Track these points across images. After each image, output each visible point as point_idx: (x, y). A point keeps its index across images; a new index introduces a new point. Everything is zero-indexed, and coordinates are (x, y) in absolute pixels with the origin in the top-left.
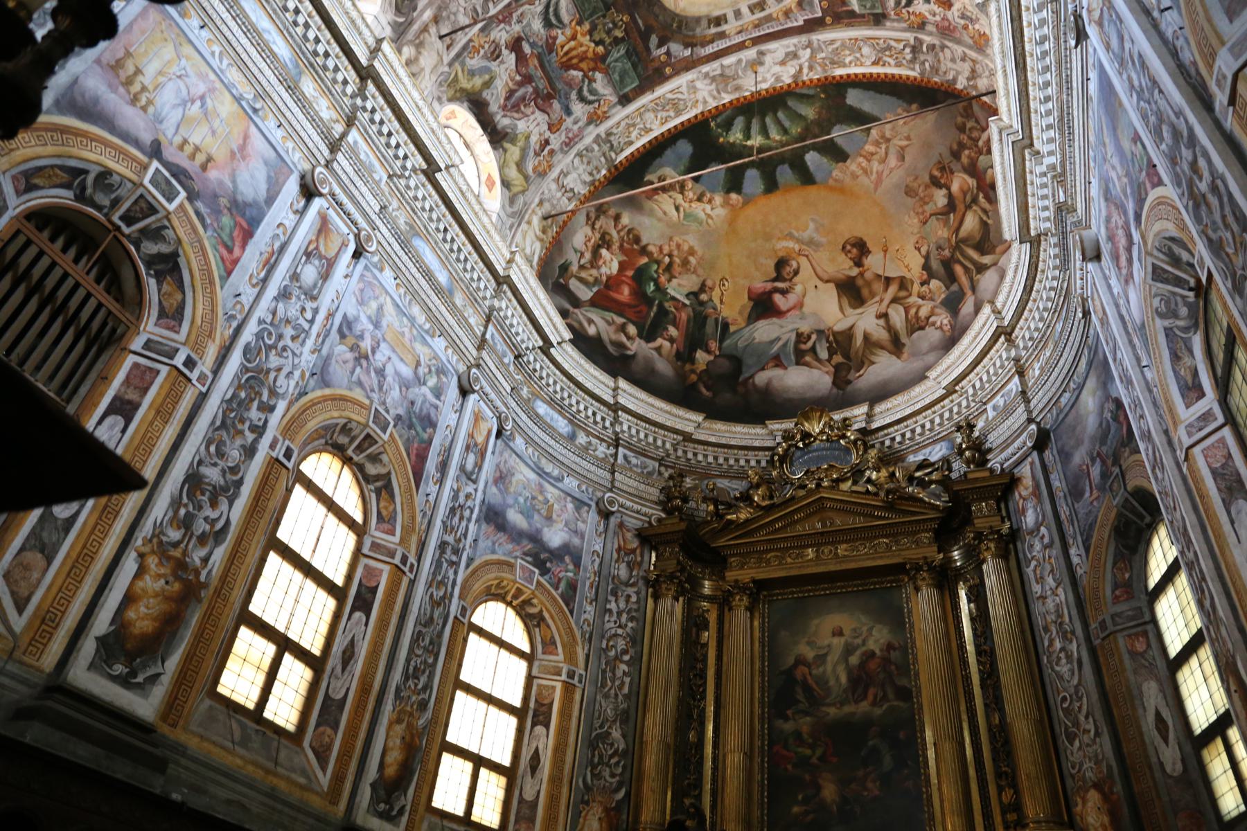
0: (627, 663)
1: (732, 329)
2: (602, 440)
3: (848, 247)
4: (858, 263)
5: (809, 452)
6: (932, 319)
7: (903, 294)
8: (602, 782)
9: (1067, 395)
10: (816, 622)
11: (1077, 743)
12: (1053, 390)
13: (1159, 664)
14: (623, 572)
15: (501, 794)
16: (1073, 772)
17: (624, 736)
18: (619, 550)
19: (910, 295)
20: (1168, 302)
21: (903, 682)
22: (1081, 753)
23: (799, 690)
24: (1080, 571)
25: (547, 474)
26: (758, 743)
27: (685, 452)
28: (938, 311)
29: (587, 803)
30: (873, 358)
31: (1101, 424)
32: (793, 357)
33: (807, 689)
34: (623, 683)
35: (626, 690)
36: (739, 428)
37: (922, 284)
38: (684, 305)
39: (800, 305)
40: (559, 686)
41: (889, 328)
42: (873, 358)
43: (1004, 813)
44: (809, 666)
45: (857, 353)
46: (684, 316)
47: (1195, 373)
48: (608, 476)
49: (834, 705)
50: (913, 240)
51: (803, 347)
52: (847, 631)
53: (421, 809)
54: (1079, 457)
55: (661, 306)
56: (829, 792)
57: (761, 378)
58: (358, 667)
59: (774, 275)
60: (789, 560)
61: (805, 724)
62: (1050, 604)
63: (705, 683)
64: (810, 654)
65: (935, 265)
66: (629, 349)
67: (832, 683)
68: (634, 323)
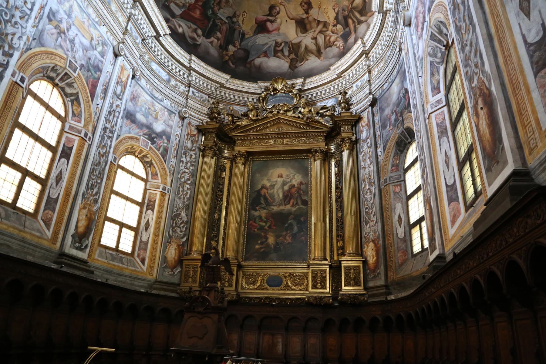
0: (189, 184)
1: (247, 36)
2: (183, 83)
3: (303, 4)
4: (307, 12)
5: (276, 97)
6: (335, 43)
7: (325, 29)
8: (177, 234)
9: (387, 84)
10: (271, 171)
11: (368, 225)
12: (382, 81)
13: (403, 197)
14: (189, 144)
15: (132, 239)
16: (365, 236)
17: (187, 215)
18: (188, 134)
19: (328, 30)
20: (434, 50)
21: (305, 198)
22: (369, 229)
23: (262, 199)
24: (380, 158)
25: (156, 98)
26: (243, 220)
27: (220, 92)
28: (339, 39)
29: (170, 243)
30: (308, 58)
31: (398, 99)
32: (273, 53)
33: (266, 199)
34: (187, 193)
35: (188, 196)
36: (246, 83)
37: (334, 26)
38: (225, 23)
39: (278, 29)
40: (159, 193)
41: (317, 44)
42: (308, 58)
43: (338, 250)
44: (267, 189)
45: (301, 54)
46: (225, 28)
47: (438, 83)
48: (185, 101)
49: (276, 205)
50: (333, 4)
51: (278, 49)
52: (284, 176)
53: (96, 245)
54: (387, 111)
55: (214, 21)
56: (271, 240)
57: (258, 61)
58: (64, 183)
59: (268, 13)
60: (263, 144)
61: (263, 213)
62: (367, 171)
63: (223, 194)
64: (268, 184)
65: (340, 18)
66: (197, 41)
67: (276, 196)
68: (201, 29)
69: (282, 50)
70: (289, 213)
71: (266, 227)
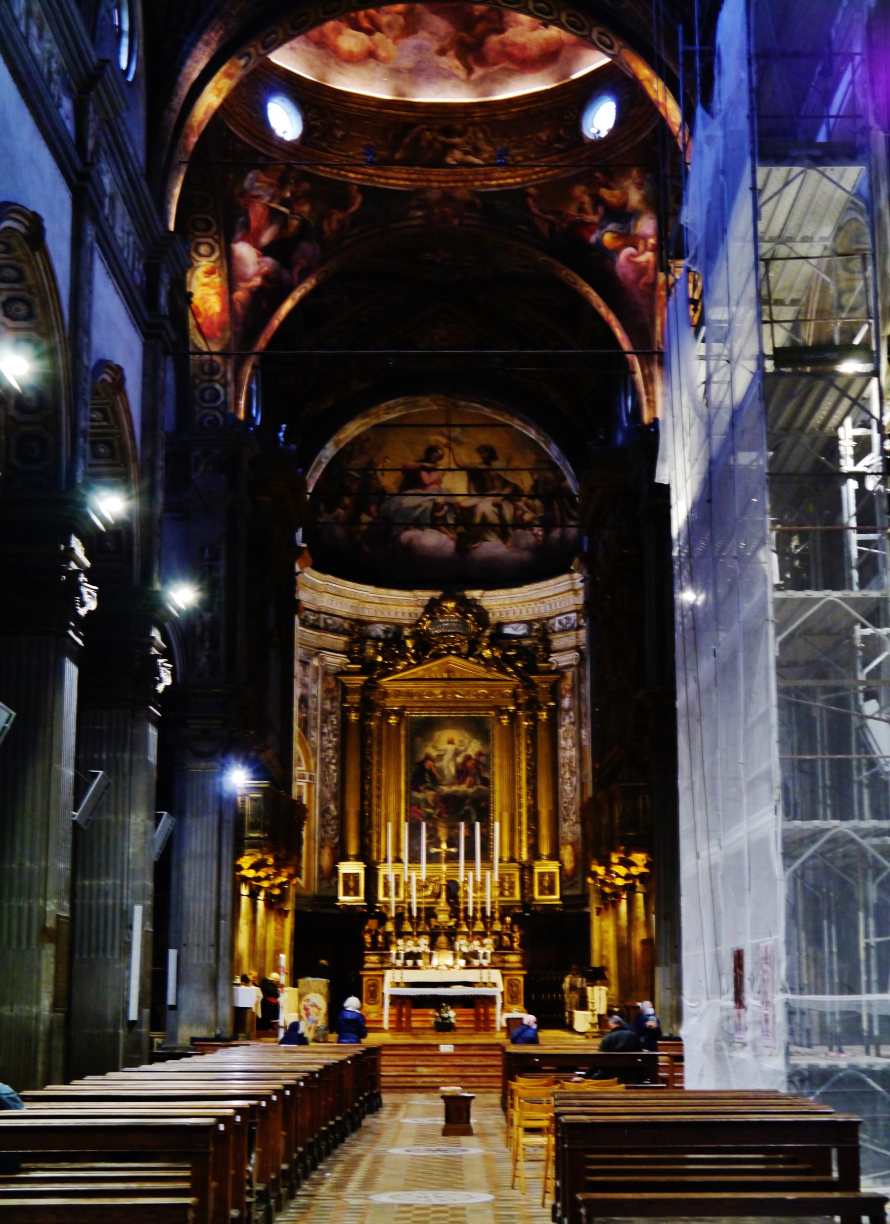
17: (336, 808)
21: (486, 775)
37: (530, 497)
39: (438, 482)
40: (305, 785)
41: (501, 515)
44: (433, 760)
52: (456, 742)
59: (423, 457)
61: (430, 795)
64: (434, 753)
67: (446, 772)
69: (444, 518)
70: (464, 797)
71: (435, 816)
